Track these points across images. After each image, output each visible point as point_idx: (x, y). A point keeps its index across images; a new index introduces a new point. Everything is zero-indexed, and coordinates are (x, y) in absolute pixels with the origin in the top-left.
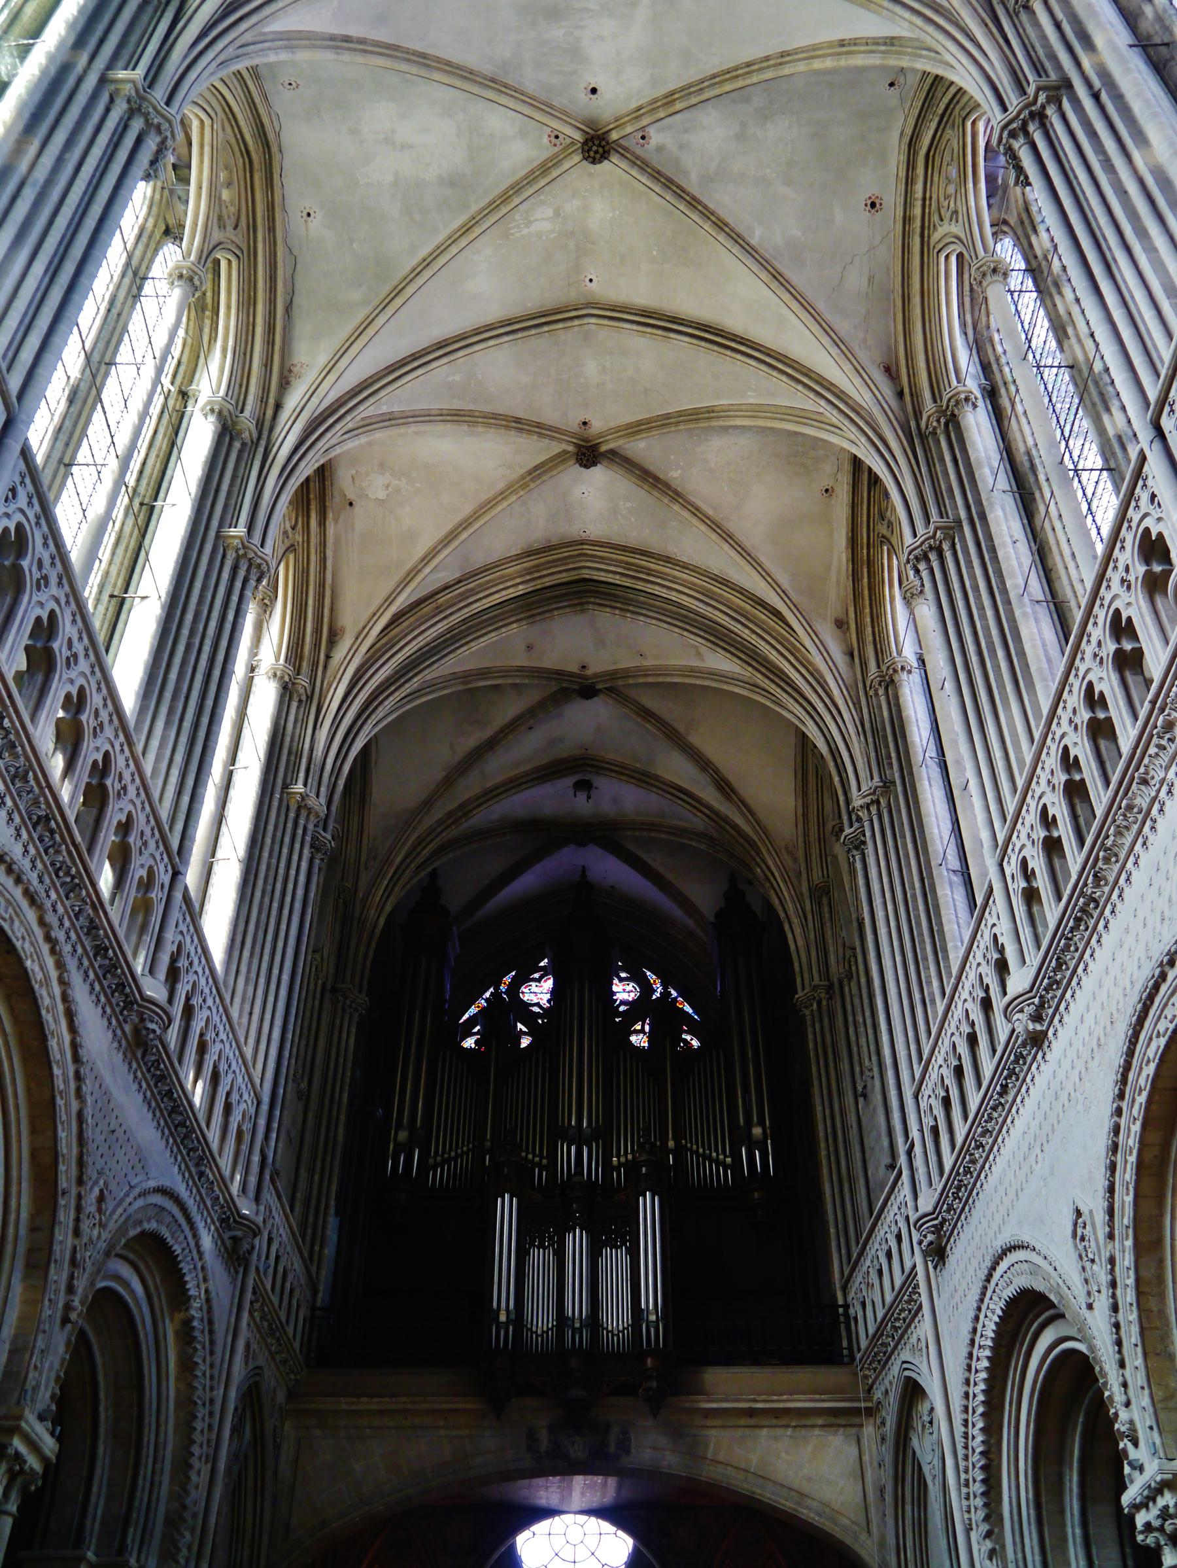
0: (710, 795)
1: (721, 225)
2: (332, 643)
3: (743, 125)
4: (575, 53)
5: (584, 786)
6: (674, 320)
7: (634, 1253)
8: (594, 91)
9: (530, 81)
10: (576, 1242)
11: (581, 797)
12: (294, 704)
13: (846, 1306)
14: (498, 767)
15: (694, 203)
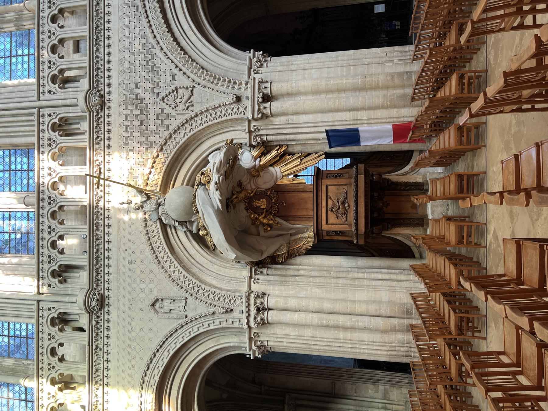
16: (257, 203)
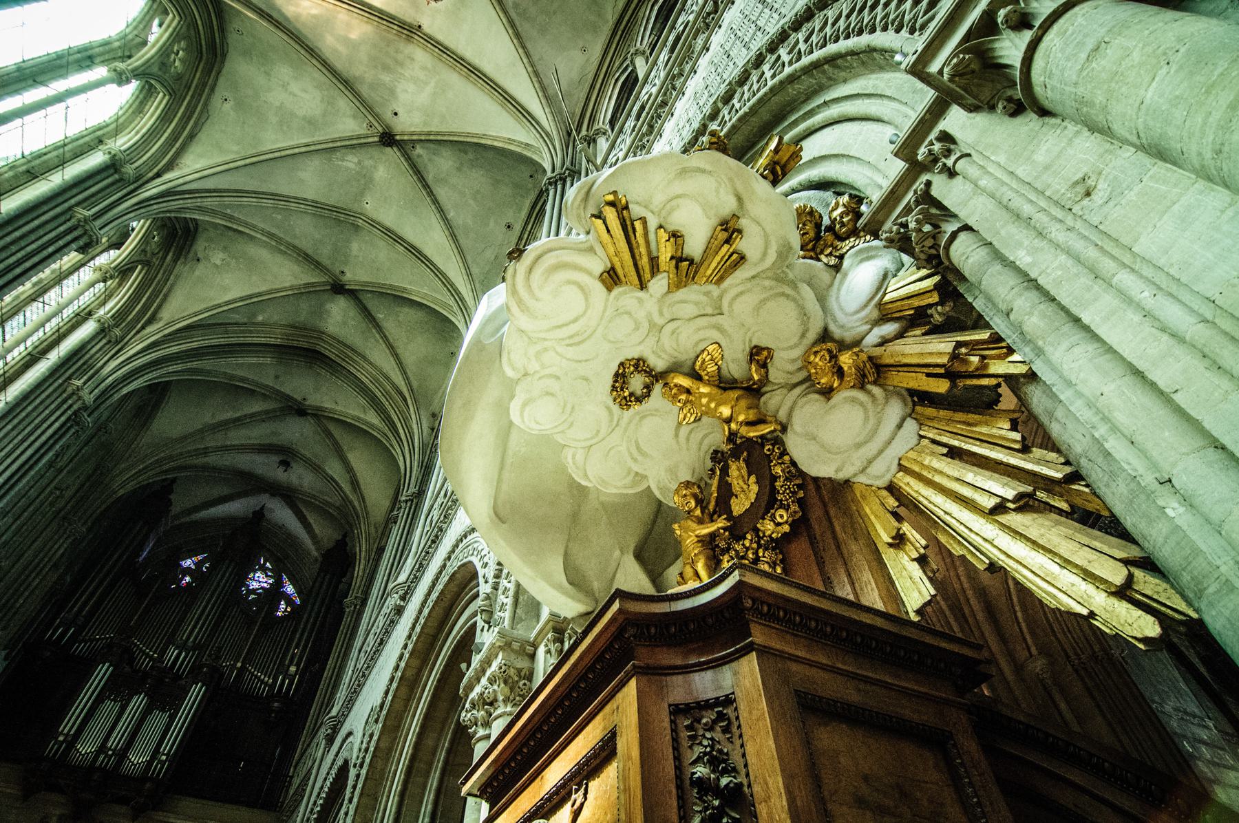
0: (347, 488)
1: (435, 201)
2: (150, 321)
3: (462, 164)
4: (392, 92)
5: (285, 464)
6: (401, 238)
7: (172, 718)
8: (396, 114)
9: (364, 91)
10: (138, 702)
11: (281, 469)
12: (104, 341)
13: (292, 777)
14: (237, 436)
15: (426, 186)
16: (736, 470)
